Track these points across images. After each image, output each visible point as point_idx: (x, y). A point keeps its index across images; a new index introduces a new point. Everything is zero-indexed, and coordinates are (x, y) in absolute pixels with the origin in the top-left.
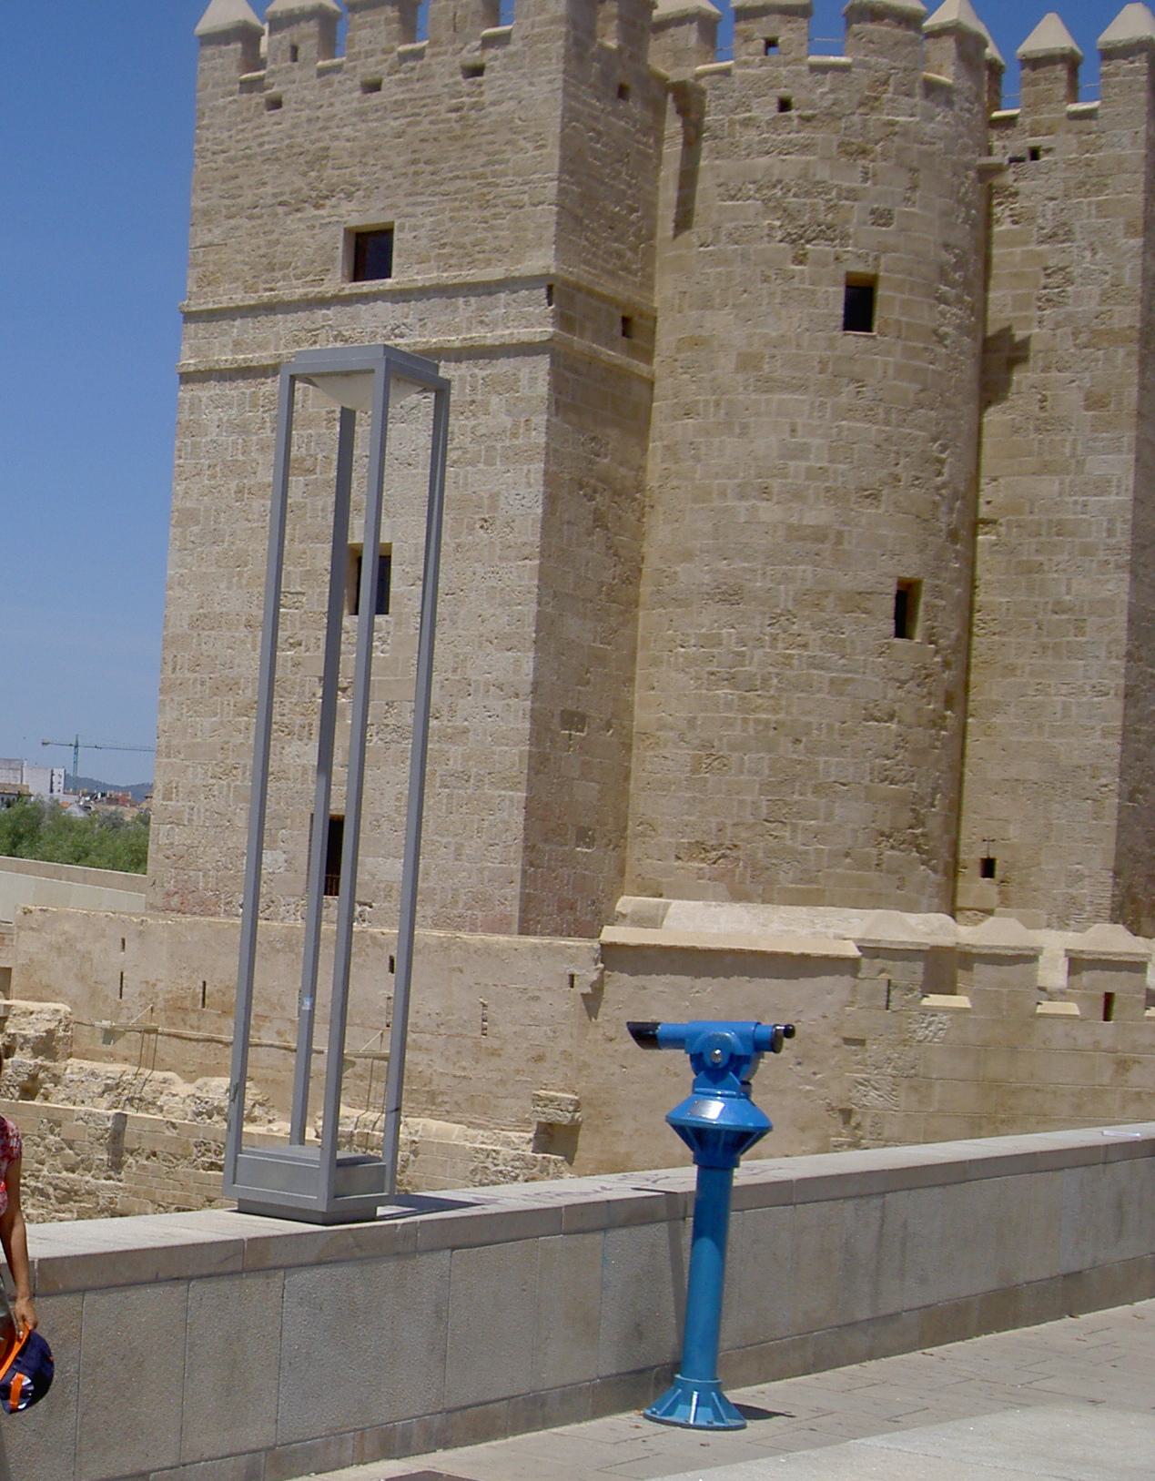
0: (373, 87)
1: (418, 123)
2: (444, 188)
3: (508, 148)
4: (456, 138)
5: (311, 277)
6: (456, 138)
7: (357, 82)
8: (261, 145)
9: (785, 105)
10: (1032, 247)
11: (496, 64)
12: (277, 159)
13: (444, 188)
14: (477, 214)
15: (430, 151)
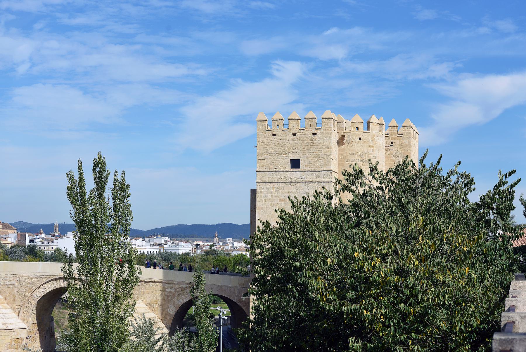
0: (294, 134)
1: (304, 142)
2: (310, 154)
3: (322, 148)
4: (311, 145)
5: (283, 167)
6: (311, 145)
7: (291, 133)
8: (272, 142)
9: (360, 139)
10: (392, 159)
11: (319, 134)
12: (275, 145)
13: (310, 154)
14: (316, 159)
15: (307, 147)
